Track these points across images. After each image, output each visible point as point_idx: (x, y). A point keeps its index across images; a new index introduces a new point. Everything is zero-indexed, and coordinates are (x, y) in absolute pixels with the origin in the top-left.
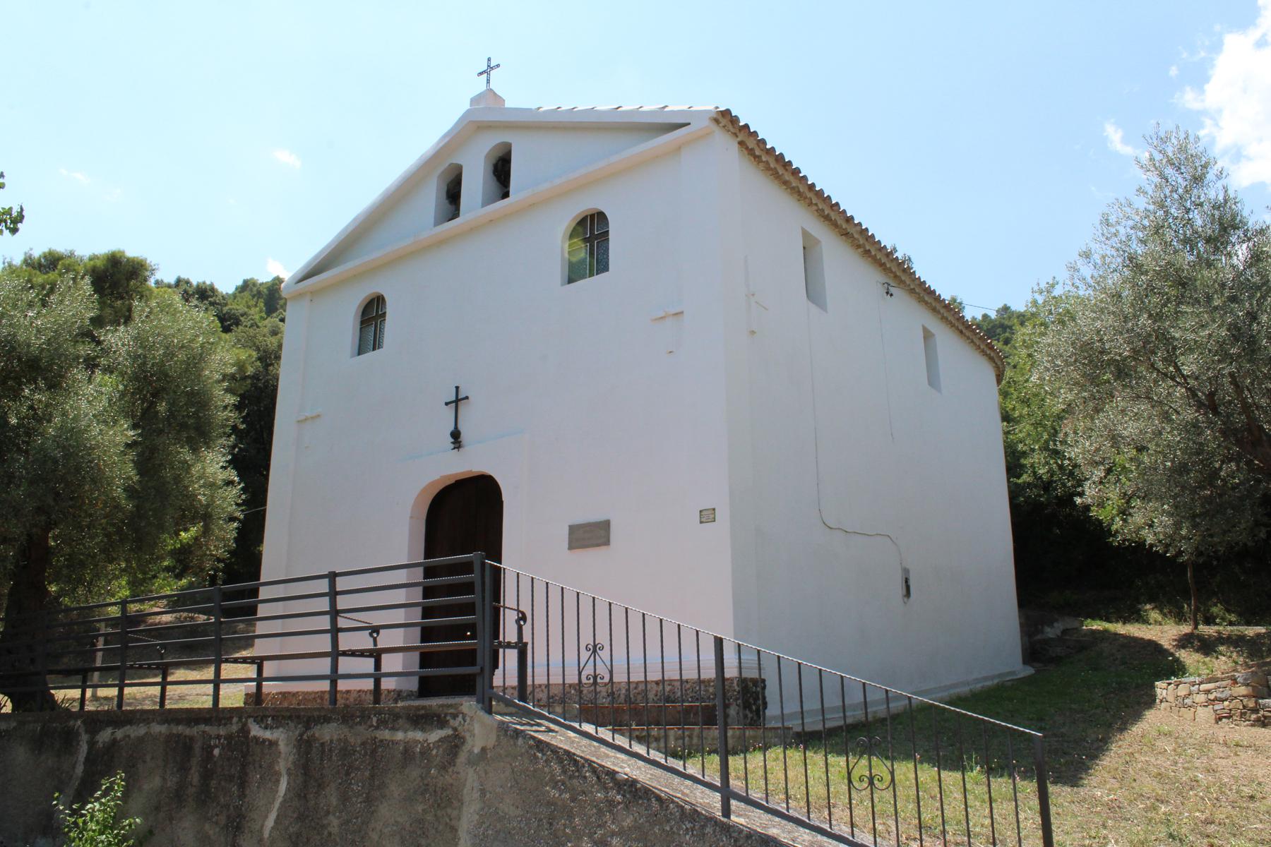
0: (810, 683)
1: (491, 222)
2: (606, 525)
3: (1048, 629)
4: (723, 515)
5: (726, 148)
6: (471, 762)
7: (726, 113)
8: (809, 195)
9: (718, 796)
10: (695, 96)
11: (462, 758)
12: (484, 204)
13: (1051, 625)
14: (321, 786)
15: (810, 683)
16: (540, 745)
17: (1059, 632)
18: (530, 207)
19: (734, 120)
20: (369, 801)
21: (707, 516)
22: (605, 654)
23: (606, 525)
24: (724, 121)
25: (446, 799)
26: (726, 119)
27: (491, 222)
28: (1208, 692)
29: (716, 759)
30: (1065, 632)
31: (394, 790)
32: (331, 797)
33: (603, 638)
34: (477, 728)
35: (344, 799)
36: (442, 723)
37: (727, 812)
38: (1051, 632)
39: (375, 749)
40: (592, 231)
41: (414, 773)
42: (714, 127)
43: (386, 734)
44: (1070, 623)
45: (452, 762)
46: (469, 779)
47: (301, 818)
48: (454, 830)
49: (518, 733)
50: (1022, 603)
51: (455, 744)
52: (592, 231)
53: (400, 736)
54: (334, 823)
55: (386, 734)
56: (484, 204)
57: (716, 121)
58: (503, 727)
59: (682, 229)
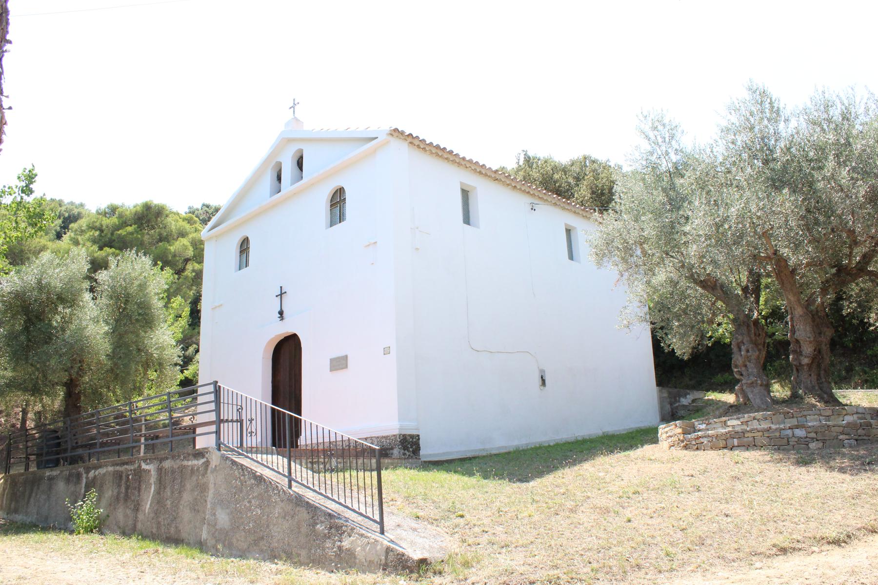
0: (326, 432)
1: (295, 194)
2: (345, 358)
3: (682, 400)
4: (393, 351)
5: (401, 148)
6: (212, 472)
7: (396, 130)
8: (463, 163)
9: (287, 479)
10: (381, 124)
11: (209, 471)
12: (271, 196)
13: (685, 396)
14: (165, 488)
15: (326, 432)
16: (234, 463)
17: (690, 401)
18: (312, 185)
19: (402, 133)
20: (180, 492)
21: (387, 351)
22: (254, 422)
23: (345, 358)
24: (396, 134)
25: (203, 488)
26: (396, 133)
27: (295, 194)
28: (667, 432)
29: (375, 474)
30: (694, 401)
31: (188, 486)
32: (168, 492)
33: (254, 417)
34: (214, 457)
35: (173, 492)
36: (203, 456)
37: (290, 487)
38: (685, 401)
39: (182, 468)
40: (338, 199)
41: (194, 478)
42: (390, 138)
43: (185, 463)
44: (697, 394)
45: (206, 473)
46: (211, 478)
47: (158, 502)
48: (206, 501)
49: (227, 458)
50: (660, 382)
51: (207, 464)
52: (338, 199)
53: (190, 463)
54: (169, 502)
55: (185, 463)
56: (271, 196)
57: (392, 135)
58: (223, 456)
59: (385, 190)
